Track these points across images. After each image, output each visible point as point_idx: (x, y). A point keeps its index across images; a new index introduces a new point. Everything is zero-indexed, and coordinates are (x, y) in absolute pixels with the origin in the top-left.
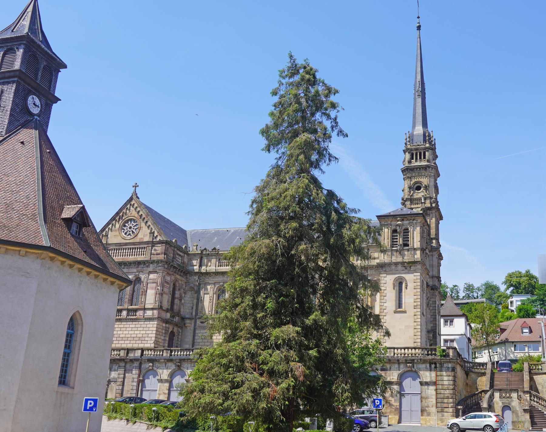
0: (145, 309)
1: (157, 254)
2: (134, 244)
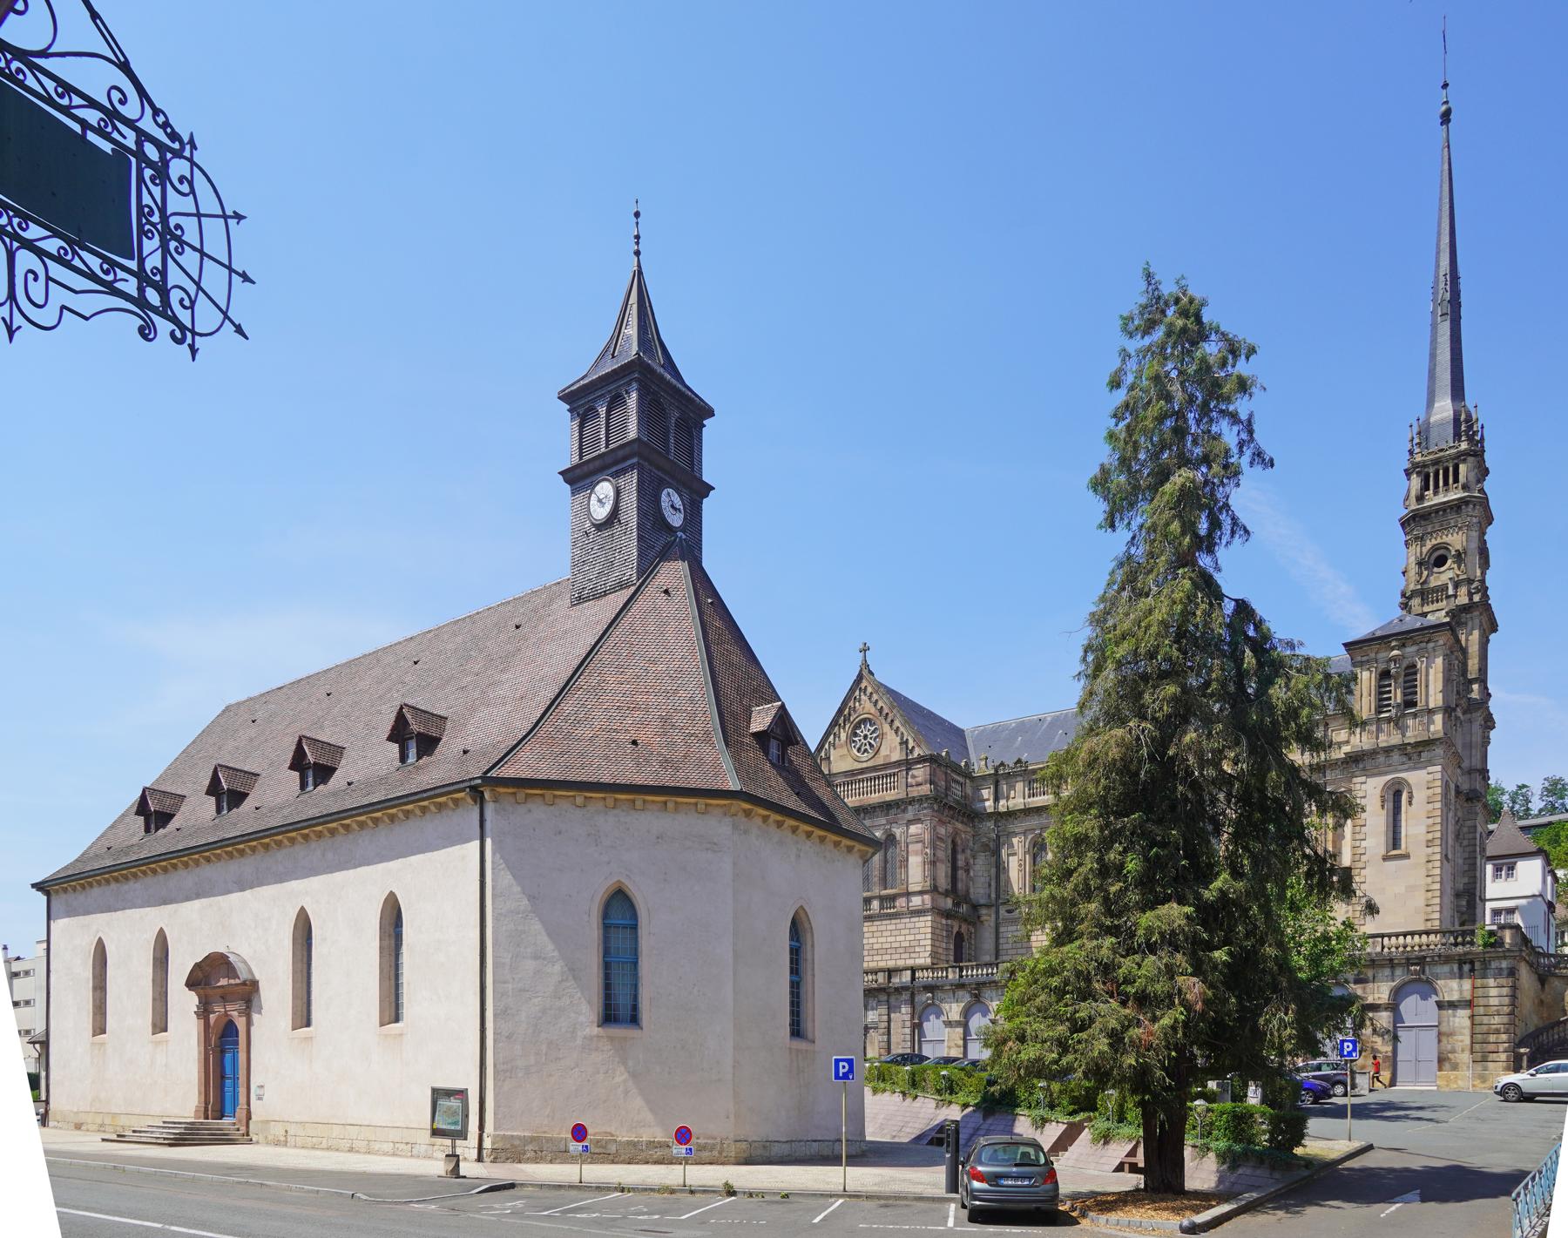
0: (908, 894)
1: (919, 785)
2: (874, 769)
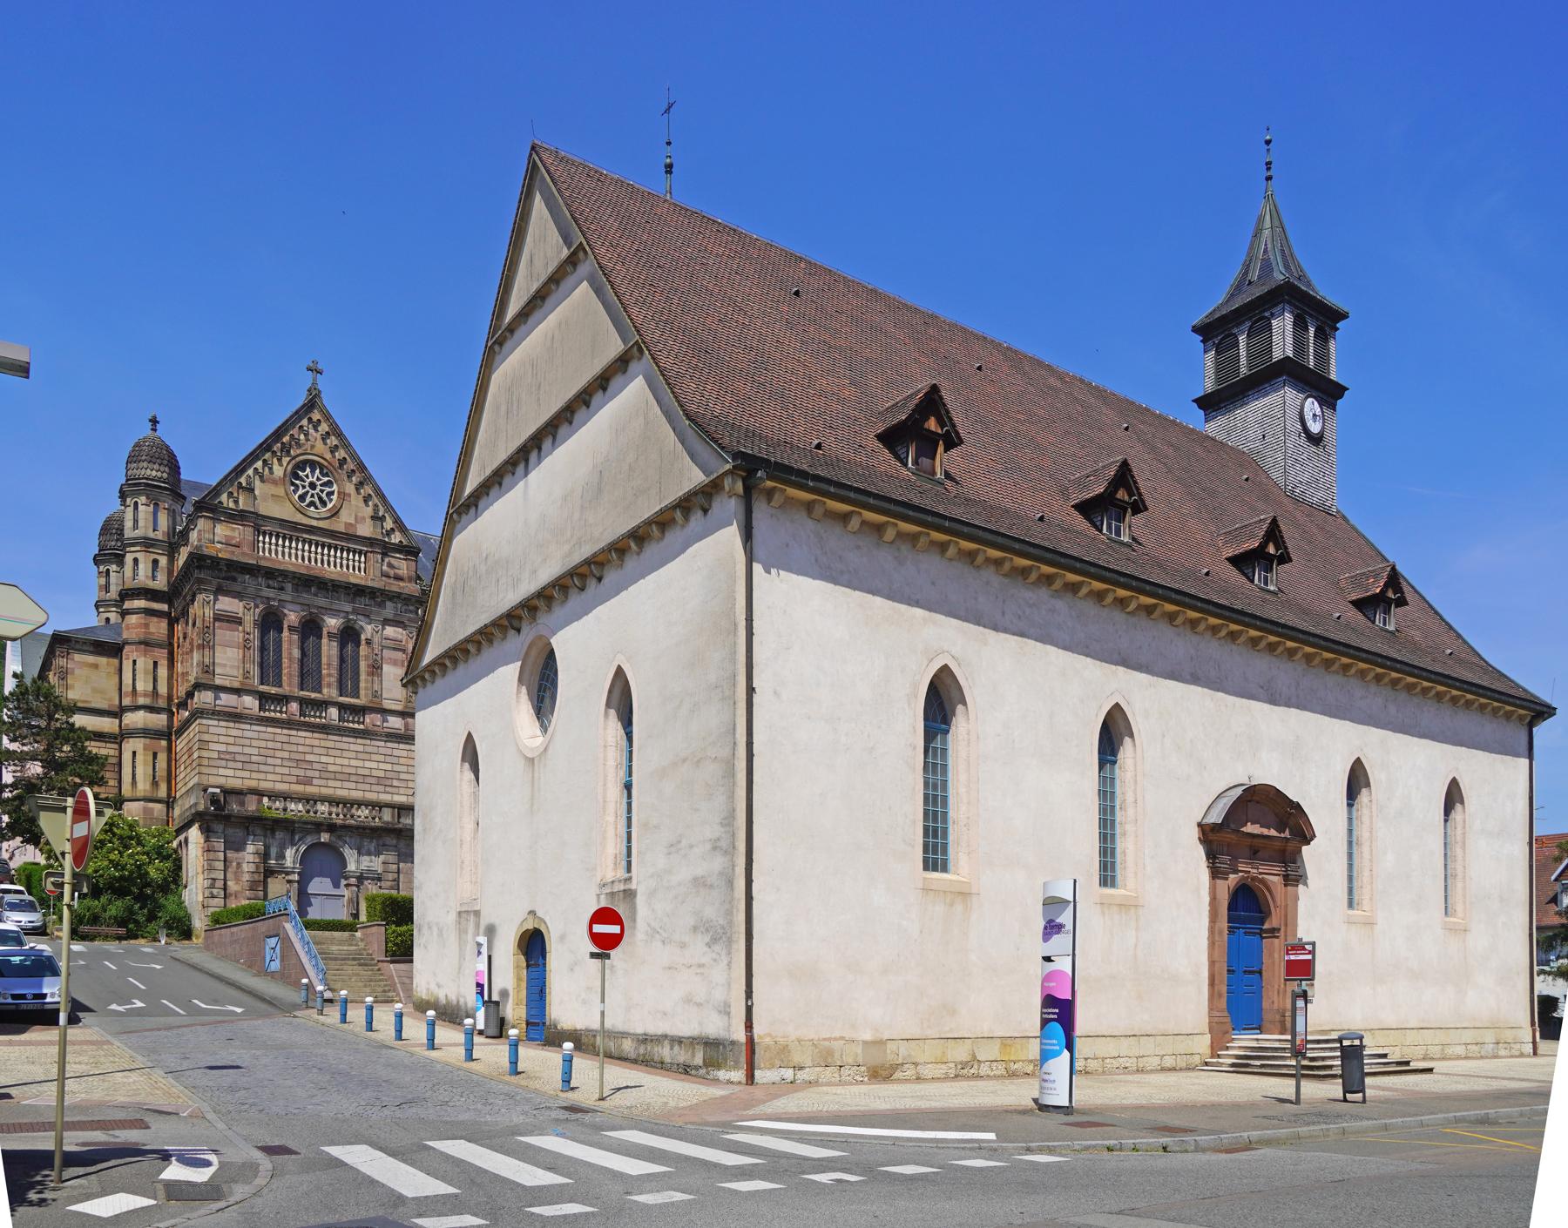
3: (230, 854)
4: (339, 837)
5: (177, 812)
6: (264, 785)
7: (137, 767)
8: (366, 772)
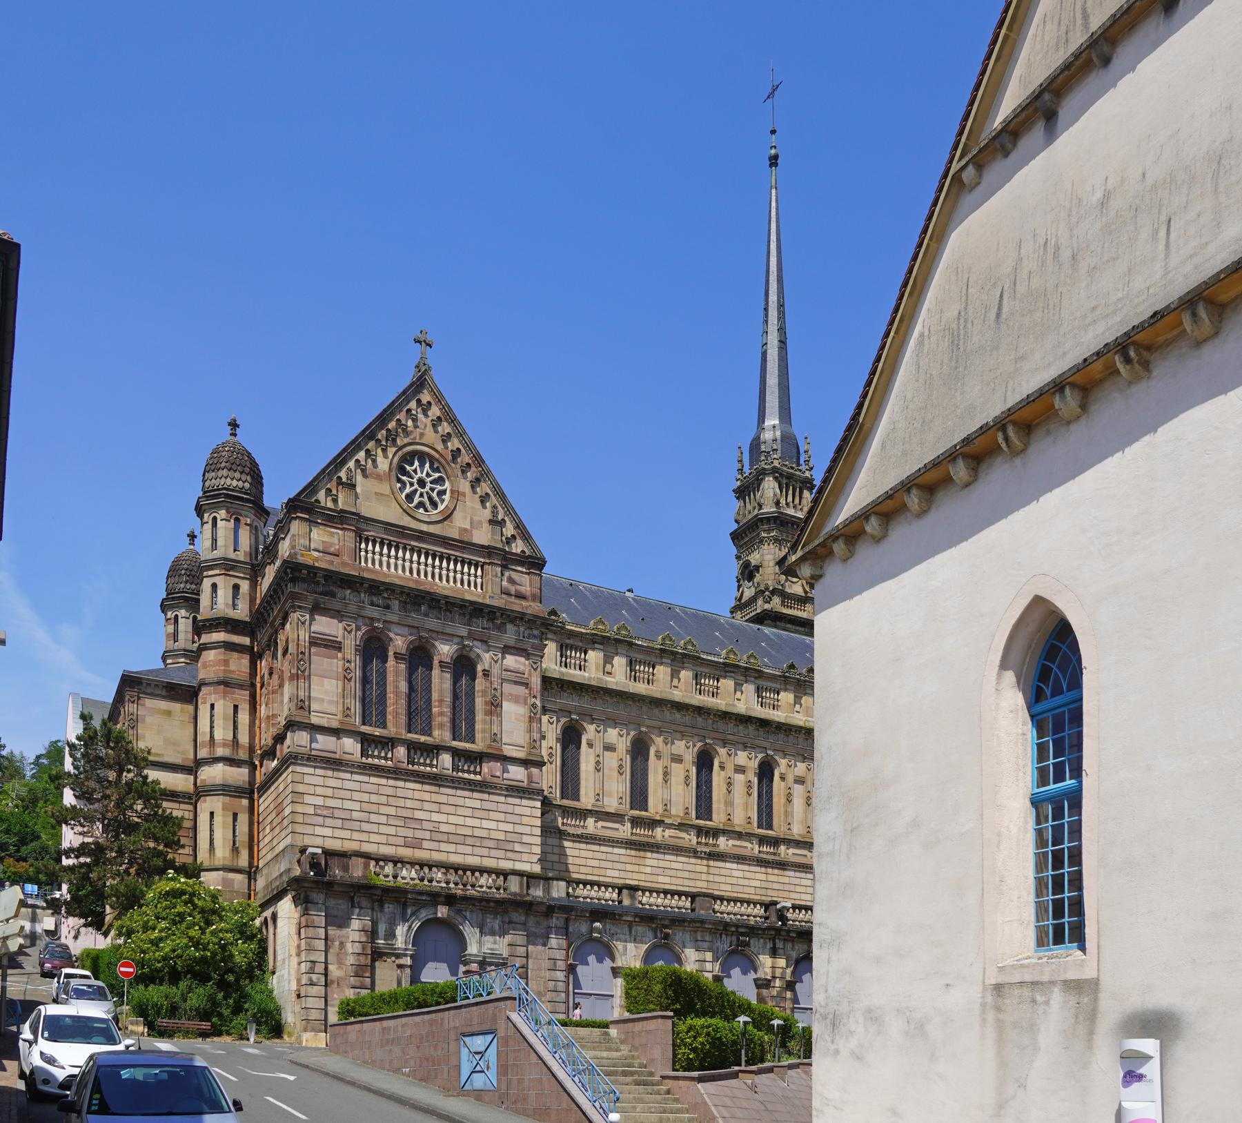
2: (444, 541)
3: (333, 931)
4: (459, 912)
5: (261, 883)
6: (367, 848)
7: (214, 833)
8: (484, 834)
